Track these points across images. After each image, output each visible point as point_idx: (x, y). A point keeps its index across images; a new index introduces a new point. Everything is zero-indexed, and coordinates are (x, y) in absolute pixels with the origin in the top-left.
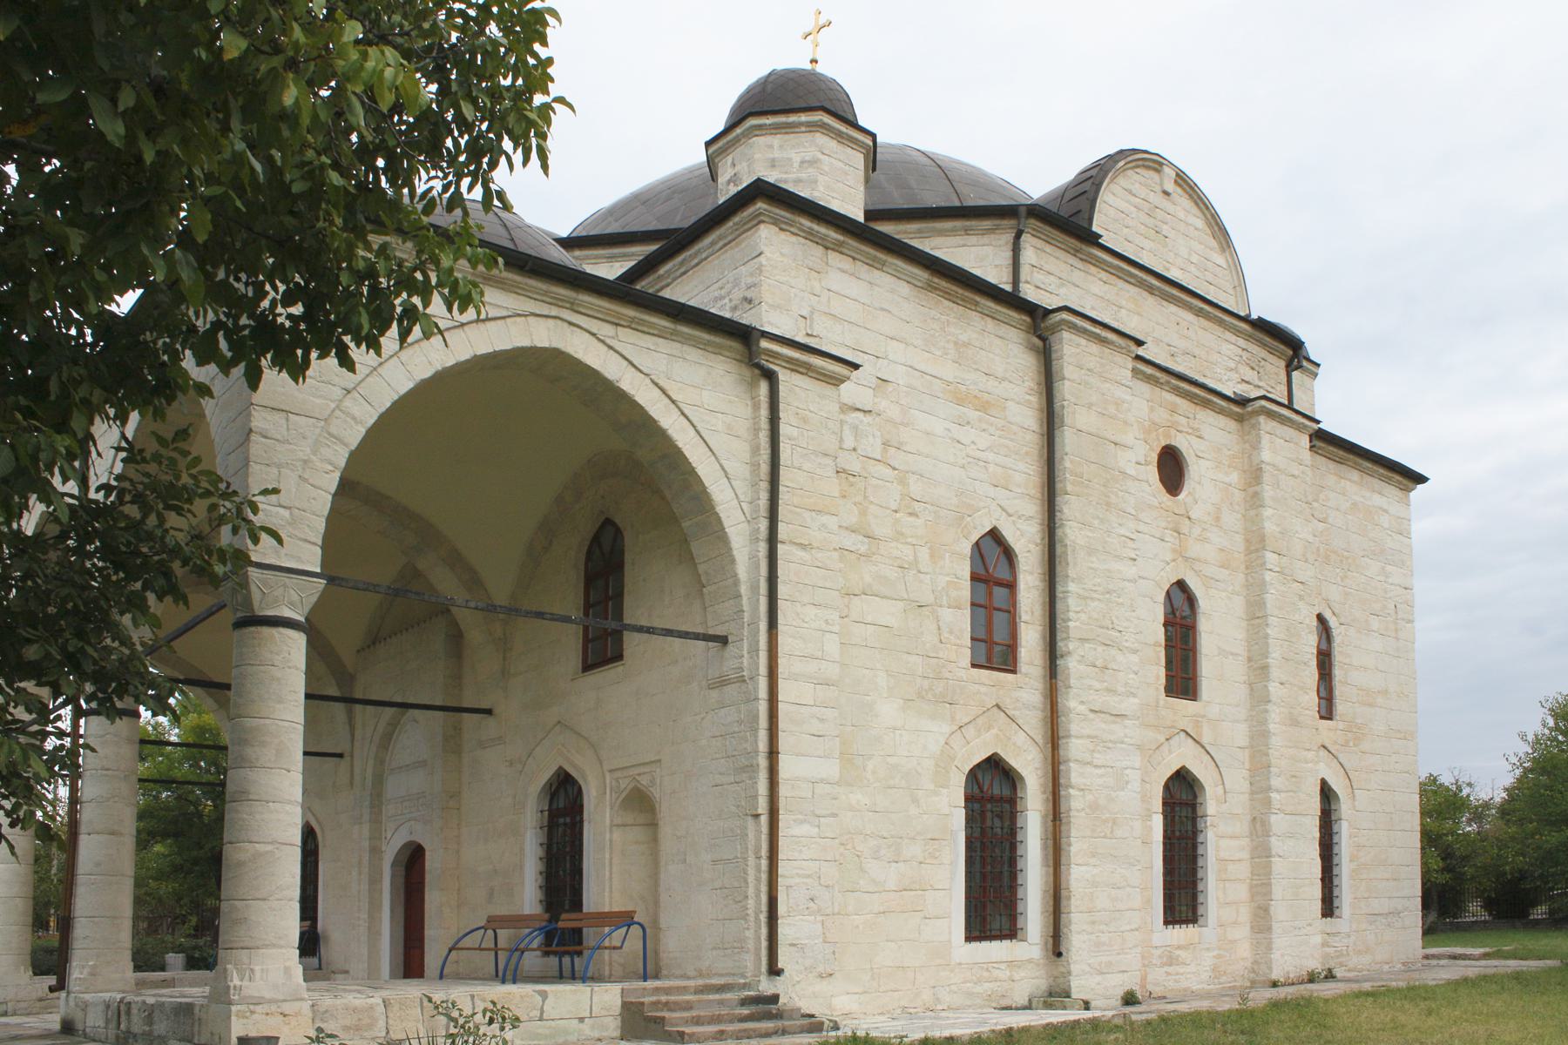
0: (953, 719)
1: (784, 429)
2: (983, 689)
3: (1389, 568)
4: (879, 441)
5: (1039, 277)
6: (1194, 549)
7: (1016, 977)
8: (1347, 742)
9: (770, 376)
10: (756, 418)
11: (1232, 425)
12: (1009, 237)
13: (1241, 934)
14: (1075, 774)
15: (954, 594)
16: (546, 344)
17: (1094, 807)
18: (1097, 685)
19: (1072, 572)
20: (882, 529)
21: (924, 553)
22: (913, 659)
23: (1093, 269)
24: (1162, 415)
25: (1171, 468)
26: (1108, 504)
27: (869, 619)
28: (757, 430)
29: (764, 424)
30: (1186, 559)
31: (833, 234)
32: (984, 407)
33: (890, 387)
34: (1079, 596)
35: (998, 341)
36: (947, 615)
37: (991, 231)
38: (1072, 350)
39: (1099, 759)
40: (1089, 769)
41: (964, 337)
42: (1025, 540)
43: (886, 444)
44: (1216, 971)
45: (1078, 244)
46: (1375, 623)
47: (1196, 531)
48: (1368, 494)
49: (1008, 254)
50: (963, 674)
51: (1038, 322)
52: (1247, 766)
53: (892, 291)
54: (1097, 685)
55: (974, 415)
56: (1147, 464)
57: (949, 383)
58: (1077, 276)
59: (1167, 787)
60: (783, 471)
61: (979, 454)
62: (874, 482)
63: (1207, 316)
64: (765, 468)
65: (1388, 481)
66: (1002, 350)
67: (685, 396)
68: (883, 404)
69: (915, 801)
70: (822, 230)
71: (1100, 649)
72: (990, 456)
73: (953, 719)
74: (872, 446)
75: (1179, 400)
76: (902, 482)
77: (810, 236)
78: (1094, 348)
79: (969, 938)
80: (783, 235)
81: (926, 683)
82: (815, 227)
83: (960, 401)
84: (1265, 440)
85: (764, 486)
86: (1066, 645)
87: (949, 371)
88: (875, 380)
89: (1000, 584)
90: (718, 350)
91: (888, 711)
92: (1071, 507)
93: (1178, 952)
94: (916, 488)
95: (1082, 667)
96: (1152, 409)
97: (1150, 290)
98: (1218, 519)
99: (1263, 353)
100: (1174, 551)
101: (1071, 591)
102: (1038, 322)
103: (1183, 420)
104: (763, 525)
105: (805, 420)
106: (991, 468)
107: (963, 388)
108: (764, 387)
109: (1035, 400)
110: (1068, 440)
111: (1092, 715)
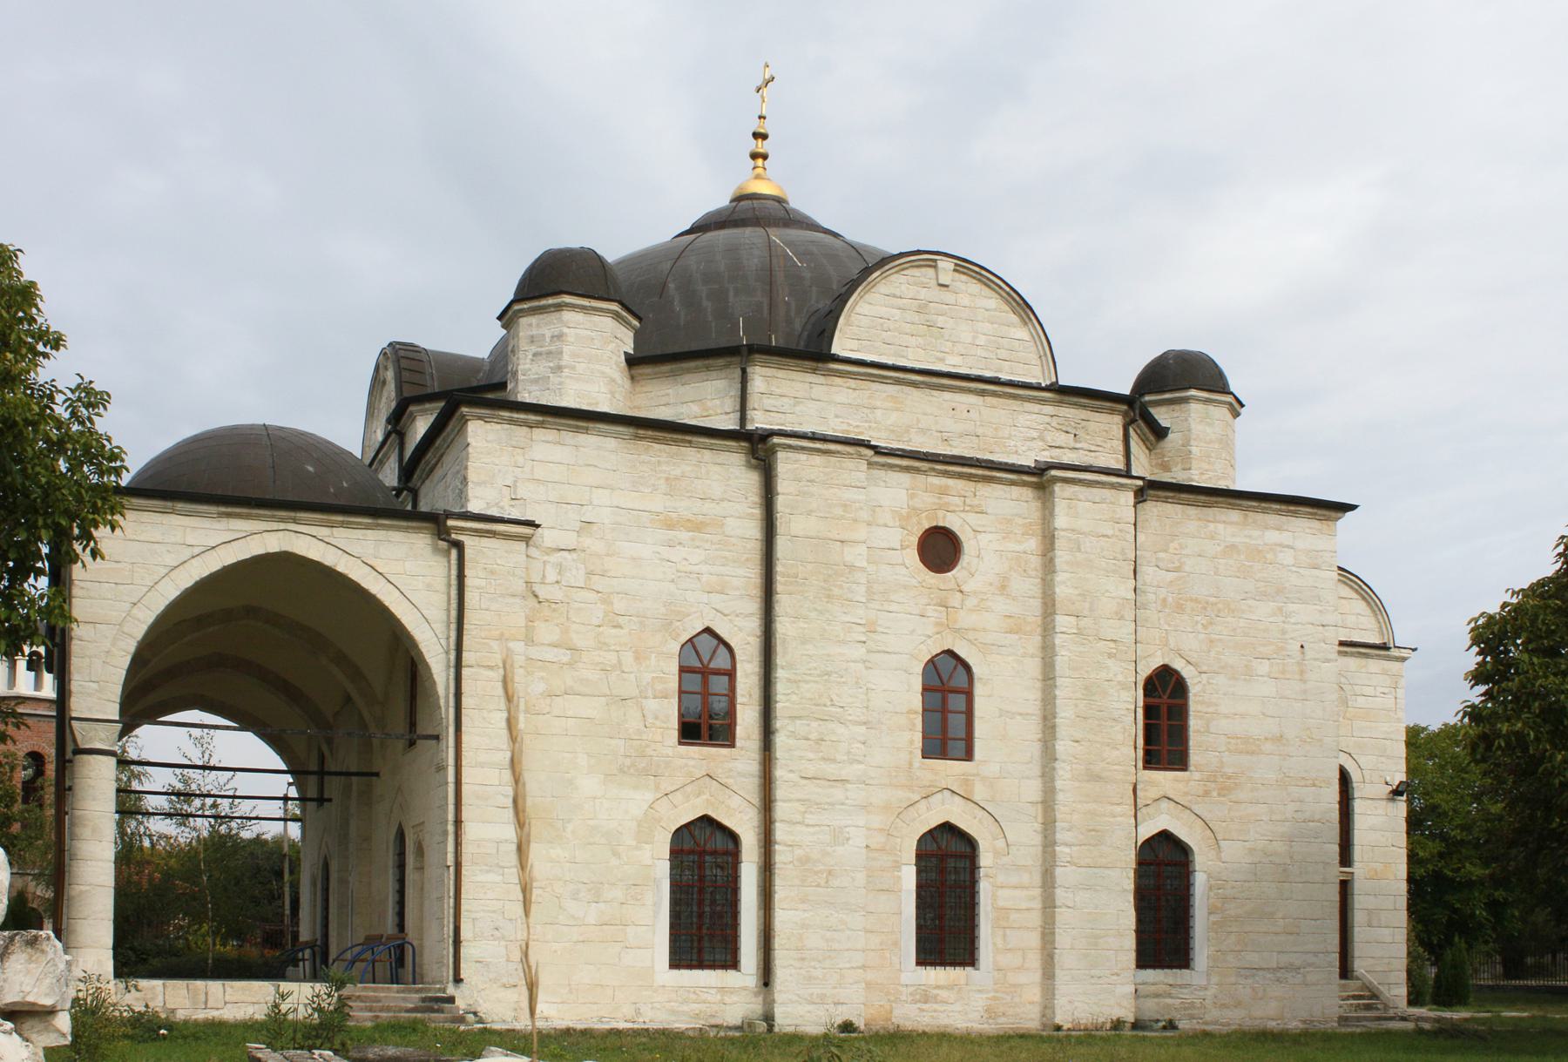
0: (657, 788)
1: (469, 581)
2: (692, 763)
3: (1292, 607)
4: (582, 572)
6: (965, 619)
7: (727, 1000)
8: (1207, 793)
9: (459, 546)
10: (449, 576)
11: (1028, 493)
12: (738, 372)
13: (1031, 979)
14: (780, 832)
15: (659, 687)
16: (276, 549)
17: (805, 860)
18: (811, 756)
20: (579, 642)
21: (628, 658)
22: (613, 742)
23: (838, 380)
24: (926, 500)
25: (940, 549)
27: (570, 713)
28: (449, 585)
29: (454, 582)
30: (957, 630)
31: (532, 417)
32: (697, 526)
33: (595, 527)
34: (789, 680)
35: (717, 468)
36: (652, 705)
37: (727, 366)
38: (788, 465)
39: (810, 819)
40: (799, 828)
41: (678, 472)
42: (743, 636)
43: (590, 573)
44: (990, 1012)
45: (814, 364)
46: (1263, 667)
47: (971, 602)
48: (1256, 533)
49: (735, 391)
50: (670, 752)
51: (759, 447)
52: (1040, 819)
53: (599, 448)
54: (811, 756)
55: (683, 535)
57: (658, 514)
58: (818, 391)
59: (919, 841)
60: (467, 613)
61: (696, 568)
62: (577, 605)
63: (994, 394)
64: (454, 613)
65: (1294, 514)
66: (730, 475)
67: (390, 567)
68: (586, 541)
69: (616, 854)
70: (522, 416)
71: (814, 724)
72: (704, 568)
73: (657, 788)
74: (576, 576)
75: (951, 482)
76: (606, 601)
77: (511, 422)
78: (818, 459)
79: (675, 963)
80: (488, 426)
81: (628, 762)
82: (515, 415)
83: (670, 525)
84: (1060, 507)
85: (453, 626)
86: (779, 723)
87: (658, 503)
88: (578, 524)
89: (718, 672)
90: (418, 530)
91: (589, 785)
93: (936, 992)
94: (619, 605)
95: (791, 742)
96: (912, 497)
99: (1084, 414)
100: (937, 624)
102: (759, 447)
104: (452, 656)
105: (492, 572)
106: (704, 578)
107: (674, 515)
108: (454, 553)
109: (757, 512)
110: (781, 544)
111: (804, 782)
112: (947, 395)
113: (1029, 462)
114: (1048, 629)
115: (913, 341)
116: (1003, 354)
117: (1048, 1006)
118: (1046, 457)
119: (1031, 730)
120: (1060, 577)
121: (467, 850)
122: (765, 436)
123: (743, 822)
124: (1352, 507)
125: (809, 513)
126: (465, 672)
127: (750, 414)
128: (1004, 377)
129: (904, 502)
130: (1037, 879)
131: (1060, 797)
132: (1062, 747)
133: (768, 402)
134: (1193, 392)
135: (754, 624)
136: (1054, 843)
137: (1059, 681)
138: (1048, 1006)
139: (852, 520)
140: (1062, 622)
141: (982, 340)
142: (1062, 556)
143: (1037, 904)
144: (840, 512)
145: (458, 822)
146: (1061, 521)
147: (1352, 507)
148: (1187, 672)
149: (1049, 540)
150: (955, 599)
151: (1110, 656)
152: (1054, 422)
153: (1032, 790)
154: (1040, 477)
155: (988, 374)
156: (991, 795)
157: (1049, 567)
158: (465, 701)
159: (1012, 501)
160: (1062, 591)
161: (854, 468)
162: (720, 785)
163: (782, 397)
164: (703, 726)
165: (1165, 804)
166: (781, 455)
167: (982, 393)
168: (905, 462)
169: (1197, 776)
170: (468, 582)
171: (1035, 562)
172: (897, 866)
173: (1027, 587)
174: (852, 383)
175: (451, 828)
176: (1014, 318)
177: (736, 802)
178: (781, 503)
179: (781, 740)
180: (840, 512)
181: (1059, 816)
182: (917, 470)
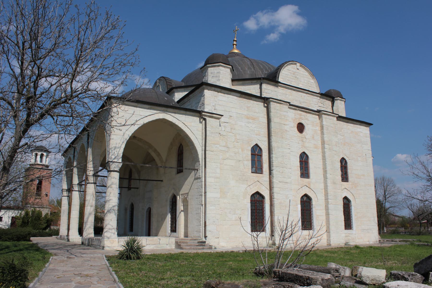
3: (363, 146)
5: (266, 91)
19: (273, 152)
26: (282, 137)
32: (254, 119)
33: (232, 117)
41: (249, 106)
51: (266, 101)
55: (251, 121)
56: (294, 127)
57: (245, 115)
61: (253, 129)
78: (278, 105)
83: (248, 118)
84: (324, 120)
92: (273, 139)
97: (294, 90)
98: (313, 138)
101: (274, 156)
102: (266, 101)
103: (303, 117)
106: (255, 131)
109: (266, 116)
112: (300, 93)
113: (316, 110)
114: (323, 148)
115: (293, 80)
116: (310, 85)
117: (329, 240)
118: (319, 109)
119: (321, 172)
120: (325, 136)
121: (208, 200)
122: (268, 99)
123: (266, 194)
124: (372, 124)
125: (278, 117)
126: (207, 152)
127: (263, 93)
128: (311, 90)
129: (293, 117)
130: (324, 208)
131: (328, 188)
132: (328, 175)
133: (266, 91)
134: (338, 98)
135: (266, 143)
136: (328, 199)
137: (327, 160)
138: (329, 240)
139: (285, 119)
140: (326, 146)
141: (306, 82)
142: (325, 131)
143: (324, 214)
144: (283, 117)
145: (205, 192)
146: (324, 123)
147: (372, 124)
148: (347, 159)
149: (322, 127)
150: (304, 140)
151: (335, 154)
152: (320, 101)
153: (322, 186)
154: (319, 112)
155: (307, 89)
156: (315, 187)
157: (322, 133)
158: (207, 160)
159: (314, 118)
160: (326, 139)
161: (285, 107)
162: (260, 183)
163: (269, 90)
164: (257, 168)
165: (345, 190)
166: (271, 103)
167: (307, 93)
168: (294, 107)
169: (350, 183)
170: (207, 129)
171: (319, 132)
172: (297, 205)
173: (319, 138)
174: (282, 88)
175: (203, 194)
176: (311, 78)
177: (264, 188)
178: (272, 114)
179: (274, 172)
180: (283, 117)
181: (329, 192)
182: (296, 110)
